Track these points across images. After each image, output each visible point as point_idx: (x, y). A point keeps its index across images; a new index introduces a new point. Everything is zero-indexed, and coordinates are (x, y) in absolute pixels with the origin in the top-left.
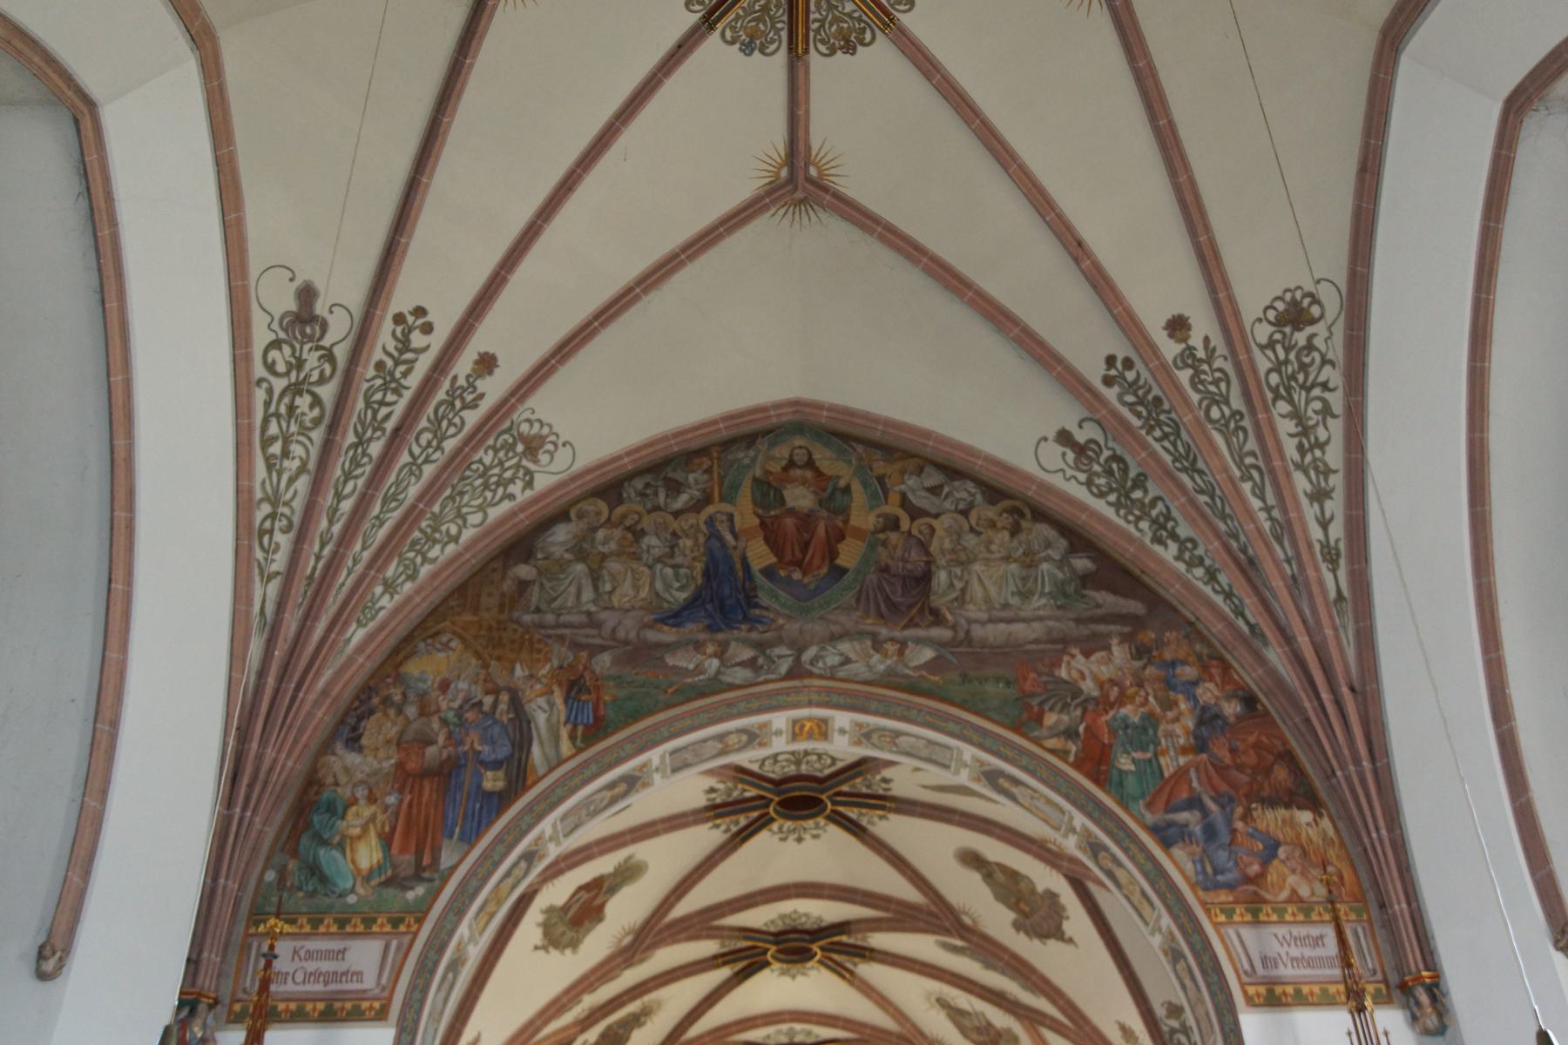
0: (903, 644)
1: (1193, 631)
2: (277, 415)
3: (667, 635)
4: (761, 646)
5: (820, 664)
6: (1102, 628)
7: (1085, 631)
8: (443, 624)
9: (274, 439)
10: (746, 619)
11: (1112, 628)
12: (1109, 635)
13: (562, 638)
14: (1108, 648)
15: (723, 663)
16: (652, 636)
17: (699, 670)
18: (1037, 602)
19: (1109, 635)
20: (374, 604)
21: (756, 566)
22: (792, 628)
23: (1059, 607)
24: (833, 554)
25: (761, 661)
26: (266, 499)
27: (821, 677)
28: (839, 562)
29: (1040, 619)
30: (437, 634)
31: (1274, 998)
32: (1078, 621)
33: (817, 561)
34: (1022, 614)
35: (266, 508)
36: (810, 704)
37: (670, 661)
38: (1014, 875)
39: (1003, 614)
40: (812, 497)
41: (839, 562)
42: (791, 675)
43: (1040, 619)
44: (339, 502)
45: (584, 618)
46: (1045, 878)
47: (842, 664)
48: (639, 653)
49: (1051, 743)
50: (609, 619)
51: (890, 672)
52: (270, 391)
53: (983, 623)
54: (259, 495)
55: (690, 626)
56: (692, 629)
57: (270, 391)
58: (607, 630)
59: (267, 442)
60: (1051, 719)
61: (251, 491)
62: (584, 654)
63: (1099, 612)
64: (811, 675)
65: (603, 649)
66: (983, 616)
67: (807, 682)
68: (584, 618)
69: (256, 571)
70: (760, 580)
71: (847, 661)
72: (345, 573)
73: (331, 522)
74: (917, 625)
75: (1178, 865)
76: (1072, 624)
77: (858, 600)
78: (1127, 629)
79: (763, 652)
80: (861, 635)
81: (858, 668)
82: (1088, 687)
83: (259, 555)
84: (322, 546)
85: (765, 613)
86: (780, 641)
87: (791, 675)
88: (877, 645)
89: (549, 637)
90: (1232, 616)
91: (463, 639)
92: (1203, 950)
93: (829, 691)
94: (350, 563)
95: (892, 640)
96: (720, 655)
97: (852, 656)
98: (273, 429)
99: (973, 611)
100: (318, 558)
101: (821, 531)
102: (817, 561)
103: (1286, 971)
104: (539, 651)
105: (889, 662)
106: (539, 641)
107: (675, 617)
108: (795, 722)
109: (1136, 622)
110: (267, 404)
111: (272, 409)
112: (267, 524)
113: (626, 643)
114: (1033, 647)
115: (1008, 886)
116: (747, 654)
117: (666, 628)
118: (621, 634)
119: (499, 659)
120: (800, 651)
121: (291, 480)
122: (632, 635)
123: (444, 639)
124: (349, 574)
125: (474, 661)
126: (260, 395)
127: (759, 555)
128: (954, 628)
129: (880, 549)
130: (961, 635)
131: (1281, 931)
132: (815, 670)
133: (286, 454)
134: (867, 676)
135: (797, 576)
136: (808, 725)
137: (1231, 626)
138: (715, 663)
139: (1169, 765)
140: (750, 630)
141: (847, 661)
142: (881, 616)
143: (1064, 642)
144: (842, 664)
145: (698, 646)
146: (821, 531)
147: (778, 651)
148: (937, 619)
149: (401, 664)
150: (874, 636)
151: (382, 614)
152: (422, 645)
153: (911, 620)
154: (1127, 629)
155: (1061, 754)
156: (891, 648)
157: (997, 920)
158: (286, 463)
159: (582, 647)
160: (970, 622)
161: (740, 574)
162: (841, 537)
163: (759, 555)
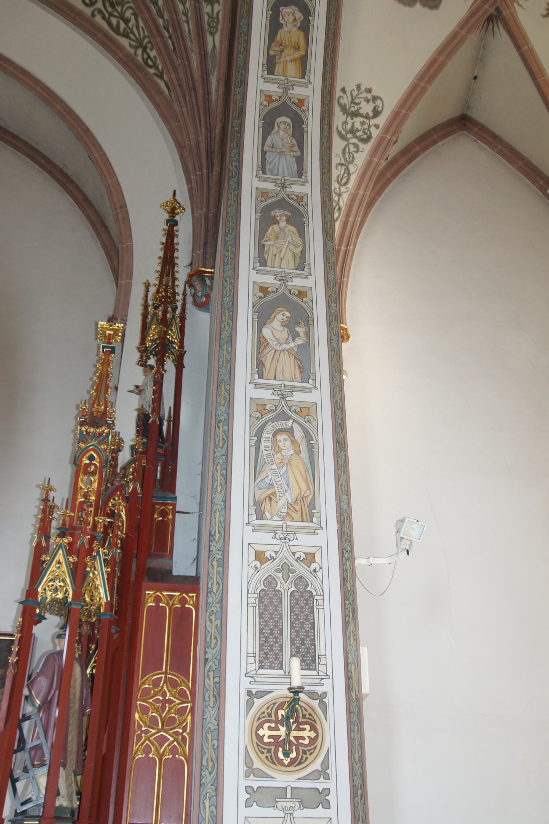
2: (111, 15)
9: (118, 24)
20: (212, 18)
26: (136, 48)
35: (140, 51)
44: (157, 5)
52: (100, 12)
54: (132, 51)
57: (100, 12)
59: (117, 31)
61: (128, 55)
69: (156, 78)
72: (186, 25)
73: (162, 17)
83: (152, 71)
84: (168, 31)
94: (184, 18)
98: (114, 21)
100: (170, 37)
110: (104, 18)
111: (107, 15)
112: (145, 56)
121: (138, 27)
124: (188, 22)
126: (98, 19)
133: (127, 22)
158: (130, 25)
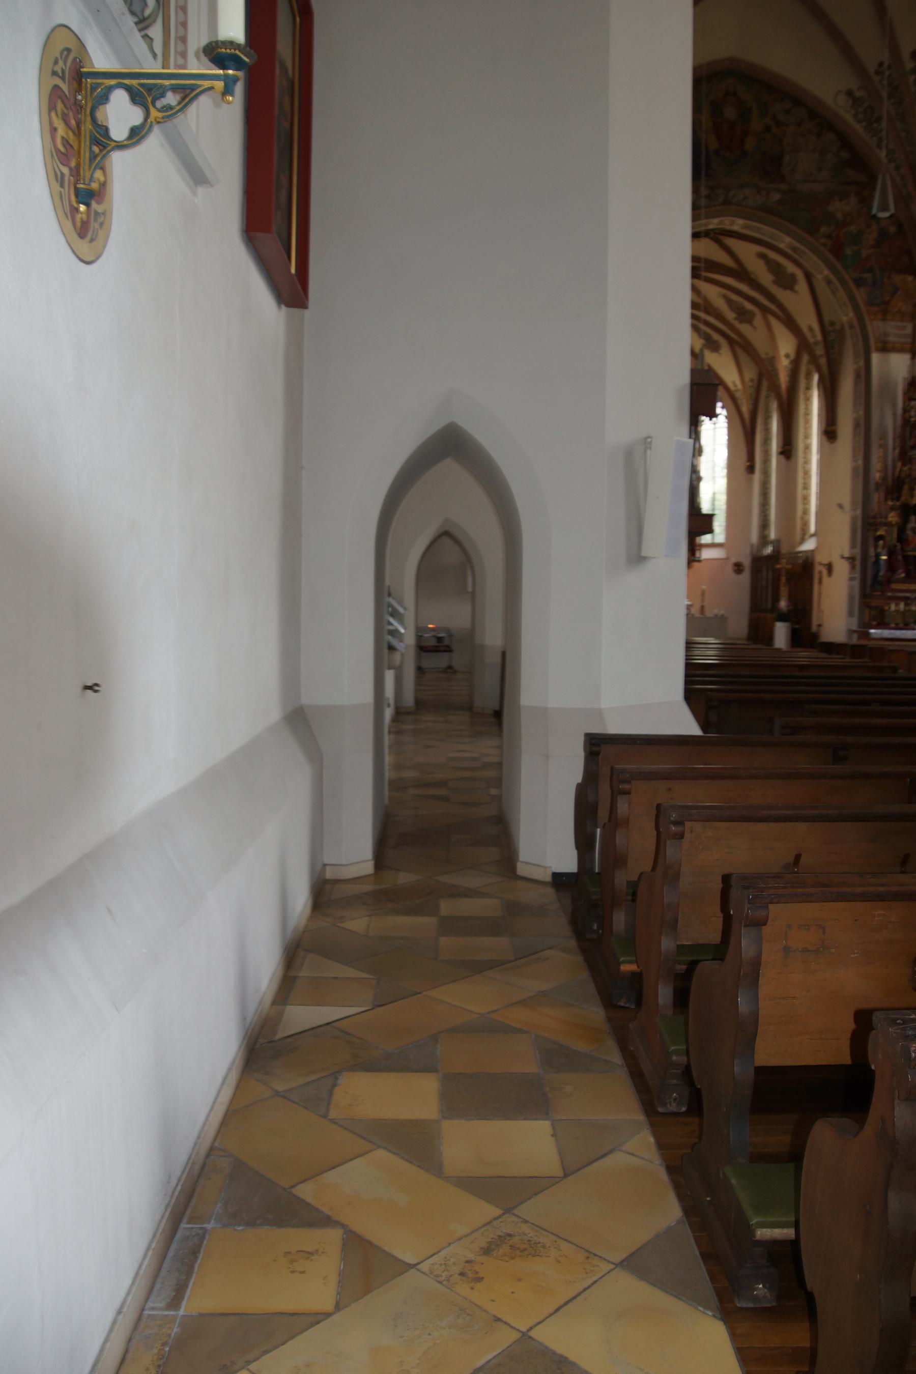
31: (885, 348)
38: (779, 265)
46: (791, 268)
49: (823, 240)
60: (824, 229)
75: (861, 295)
82: (839, 215)
92: (863, 329)
103: (891, 339)
115: (775, 269)
131: (892, 323)
139: (865, 253)
155: (824, 245)
157: (766, 278)
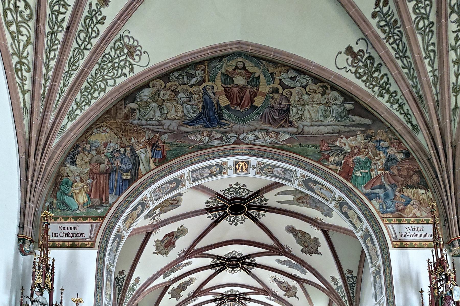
0: (278, 133)
1: (389, 129)
3: (189, 129)
4: (224, 133)
5: (246, 139)
6: (354, 128)
7: (347, 129)
8: (103, 124)
10: (218, 124)
11: (358, 128)
12: (357, 131)
13: (149, 129)
14: (356, 136)
15: (210, 139)
16: (183, 129)
17: (201, 141)
18: (330, 119)
19: (357, 131)
21: (222, 105)
22: (236, 127)
23: (338, 121)
24: (252, 101)
25: (224, 138)
27: (247, 144)
28: (254, 104)
29: (331, 125)
30: (101, 127)
32: (345, 126)
33: (246, 104)
34: (324, 123)
36: (242, 154)
37: (190, 137)
39: (317, 123)
40: (245, 80)
41: (254, 104)
42: (235, 143)
43: (331, 125)
45: (157, 122)
47: (255, 140)
48: (177, 134)
50: (167, 123)
51: (272, 142)
53: (308, 126)
55: (197, 126)
56: (198, 127)
58: (166, 127)
62: (158, 135)
63: (354, 123)
64: (243, 143)
65: (165, 133)
66: (309, 124)
67: (241, 145)
68: (157, 122)
70: (224, 110)
71: (257, 139)
74: (283, 127)
76: (343, 127)
77: (261, 118)
78: (363, 129)
79: (225, 136)
80: (262, 130)
81: (261, 141)
85: (226, 122)
86: (232, 131)
87: (235, 143)
88: (268, 133)
89: (144, 129)
90: (406, 123)
91: (111, 129)
93: (250, 149)
95: (274, 132)
96: (209, 136)
97: (259, 137)
99: (305, 122)
101: (248, 93)
102: (246, 104)
104: (140, 133)
105: (272, 139)
106: (140, 130)
107: (192, 123)
108: (237, 162)
109: (368, 127)
113: (174, 131)
114: (327, 135)
116: (219, 136)
117: (188, 126)
118: (171, 128)
119: (125, 136)
120: (239, 135)
122: (176, 128)
123: (104, 129)
125: (116, 137)
127: (224, 101)
128: (297, 128)
129: (270, 100)
130: (300, 130)
132: (244, 141)
134: (264, 144)
135: (238, 109)
136: (241, 164)
137: (405, 127)
138: (207, 138)
140: (220, 128)
141: (257, 139)
142: (270, 123)
143: (339, 133)
144: (255, 140)
145: (200, 133)
146: (248, 93)
147: (230, 135)
148: (291, 124)
149: (88, 137)
150: (267, 130)
151: (78, 117)
152: (95, 130)
153: (281, 125)
154: (363, 129)
156: (273, 134)
159: (157, 132)
160: (303, 126)
161: (216, 108)
162: (256, 95)
163: (224, 101)
